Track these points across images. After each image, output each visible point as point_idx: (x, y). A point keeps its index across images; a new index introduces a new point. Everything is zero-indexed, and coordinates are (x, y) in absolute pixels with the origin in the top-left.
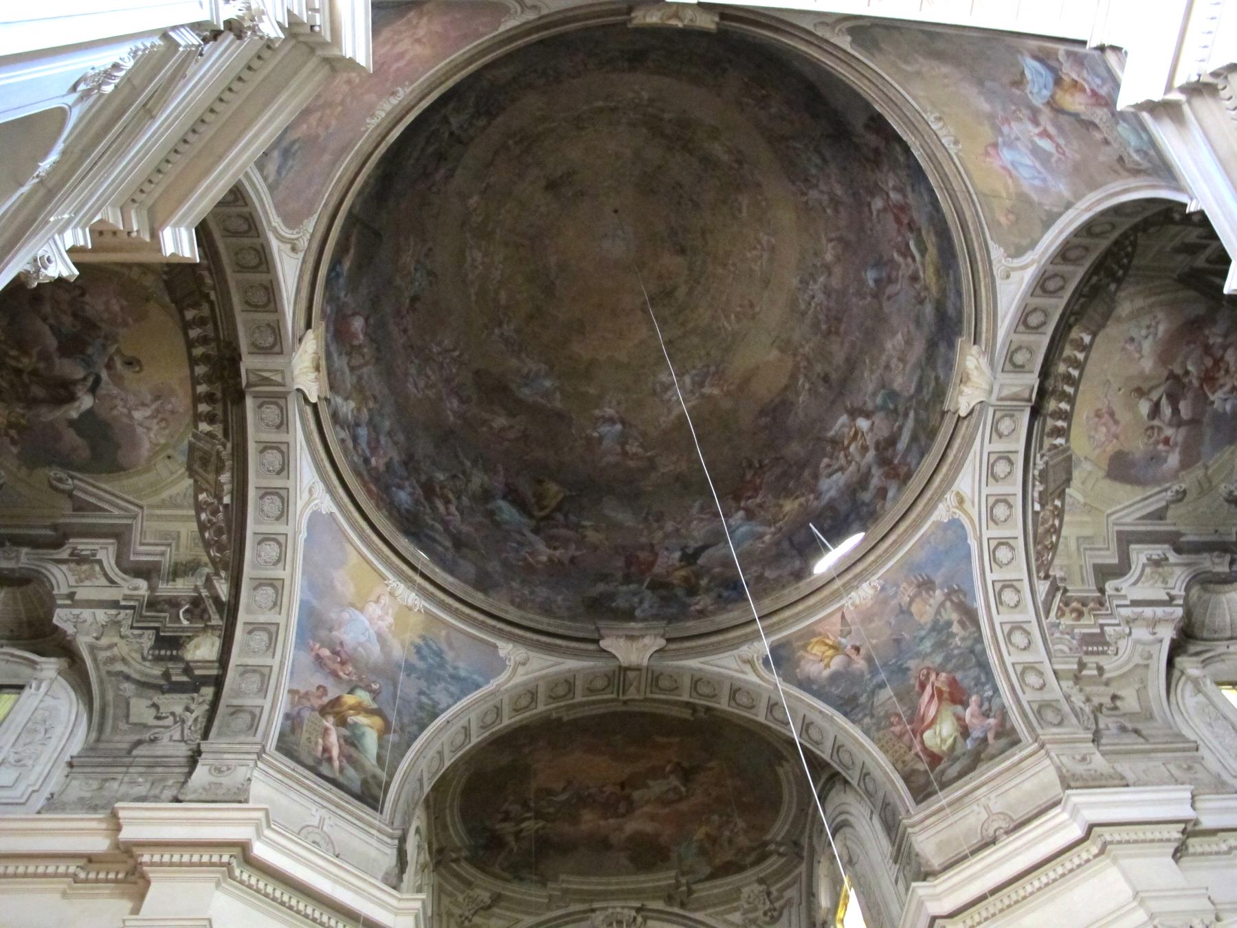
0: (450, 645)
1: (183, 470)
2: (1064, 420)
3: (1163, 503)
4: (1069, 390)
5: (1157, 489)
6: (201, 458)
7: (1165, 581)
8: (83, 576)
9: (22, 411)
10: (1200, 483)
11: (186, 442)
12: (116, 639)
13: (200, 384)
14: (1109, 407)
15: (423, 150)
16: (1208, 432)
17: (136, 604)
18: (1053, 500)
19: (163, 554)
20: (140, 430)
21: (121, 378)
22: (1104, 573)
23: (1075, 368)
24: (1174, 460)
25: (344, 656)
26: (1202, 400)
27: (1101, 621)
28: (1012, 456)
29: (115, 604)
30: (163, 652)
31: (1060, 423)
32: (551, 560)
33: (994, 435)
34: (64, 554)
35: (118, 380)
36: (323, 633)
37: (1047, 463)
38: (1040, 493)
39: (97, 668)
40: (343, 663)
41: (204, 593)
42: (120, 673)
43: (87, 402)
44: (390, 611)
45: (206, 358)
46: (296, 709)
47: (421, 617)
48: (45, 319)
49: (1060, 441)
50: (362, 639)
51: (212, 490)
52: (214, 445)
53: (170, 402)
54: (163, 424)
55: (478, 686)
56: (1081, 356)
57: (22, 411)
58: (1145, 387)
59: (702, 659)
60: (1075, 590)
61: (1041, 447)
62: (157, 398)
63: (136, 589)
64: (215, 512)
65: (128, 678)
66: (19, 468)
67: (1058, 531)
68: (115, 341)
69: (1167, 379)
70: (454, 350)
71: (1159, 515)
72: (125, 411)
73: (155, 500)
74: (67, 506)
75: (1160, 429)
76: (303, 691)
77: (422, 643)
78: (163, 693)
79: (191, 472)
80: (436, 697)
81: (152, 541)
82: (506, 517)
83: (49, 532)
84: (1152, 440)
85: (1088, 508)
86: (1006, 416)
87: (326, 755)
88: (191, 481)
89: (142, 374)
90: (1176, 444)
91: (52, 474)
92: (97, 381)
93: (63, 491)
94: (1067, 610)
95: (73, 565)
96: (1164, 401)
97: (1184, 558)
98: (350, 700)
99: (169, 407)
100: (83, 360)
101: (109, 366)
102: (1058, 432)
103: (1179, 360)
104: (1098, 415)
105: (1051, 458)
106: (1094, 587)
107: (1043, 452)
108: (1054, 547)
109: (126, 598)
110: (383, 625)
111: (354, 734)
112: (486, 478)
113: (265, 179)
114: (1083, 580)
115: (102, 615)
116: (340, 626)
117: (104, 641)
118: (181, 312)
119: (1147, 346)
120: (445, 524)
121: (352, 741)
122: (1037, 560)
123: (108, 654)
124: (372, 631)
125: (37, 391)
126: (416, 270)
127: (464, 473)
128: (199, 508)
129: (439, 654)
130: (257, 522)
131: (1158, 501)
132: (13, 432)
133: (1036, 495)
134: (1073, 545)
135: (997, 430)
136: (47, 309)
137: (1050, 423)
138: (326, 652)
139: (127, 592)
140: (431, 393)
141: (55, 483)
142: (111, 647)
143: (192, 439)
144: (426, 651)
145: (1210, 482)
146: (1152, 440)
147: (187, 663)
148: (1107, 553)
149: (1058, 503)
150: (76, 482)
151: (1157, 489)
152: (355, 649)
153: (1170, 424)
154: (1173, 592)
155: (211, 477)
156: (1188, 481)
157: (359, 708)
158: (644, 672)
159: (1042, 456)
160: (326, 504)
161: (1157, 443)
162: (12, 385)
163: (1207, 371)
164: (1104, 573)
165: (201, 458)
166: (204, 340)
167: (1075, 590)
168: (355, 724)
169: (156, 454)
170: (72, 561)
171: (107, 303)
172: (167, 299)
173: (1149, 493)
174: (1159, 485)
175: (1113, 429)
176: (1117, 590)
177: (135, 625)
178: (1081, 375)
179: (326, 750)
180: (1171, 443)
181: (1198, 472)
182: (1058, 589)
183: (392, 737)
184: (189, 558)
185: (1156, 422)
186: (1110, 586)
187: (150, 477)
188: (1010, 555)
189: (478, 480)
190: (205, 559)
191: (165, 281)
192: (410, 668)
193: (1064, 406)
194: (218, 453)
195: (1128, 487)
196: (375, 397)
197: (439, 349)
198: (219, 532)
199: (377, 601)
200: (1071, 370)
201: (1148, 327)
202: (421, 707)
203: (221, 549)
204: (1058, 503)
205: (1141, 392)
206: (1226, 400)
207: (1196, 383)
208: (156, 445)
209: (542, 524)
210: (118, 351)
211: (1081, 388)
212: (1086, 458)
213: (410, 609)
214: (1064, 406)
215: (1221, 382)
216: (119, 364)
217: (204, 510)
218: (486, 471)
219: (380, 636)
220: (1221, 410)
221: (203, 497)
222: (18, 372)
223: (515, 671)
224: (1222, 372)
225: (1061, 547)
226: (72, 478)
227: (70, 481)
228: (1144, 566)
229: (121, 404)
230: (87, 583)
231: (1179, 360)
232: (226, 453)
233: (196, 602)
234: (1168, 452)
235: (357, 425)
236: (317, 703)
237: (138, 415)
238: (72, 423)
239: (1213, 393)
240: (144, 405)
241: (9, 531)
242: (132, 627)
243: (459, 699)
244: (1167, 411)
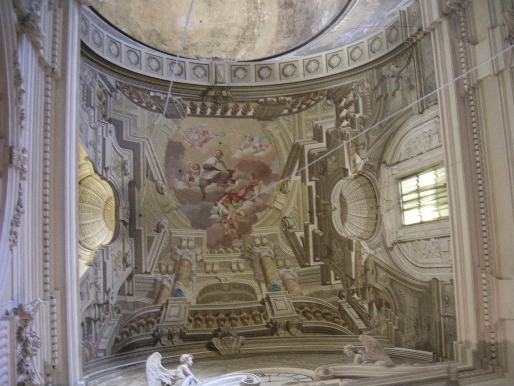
2: (201, 112)
3: (156, 178)
4: (218, 113)
5: (163, 175)
7: (114, 169)
10: (167, 205)
14: (210, 138)
16: (197, 207)
18: (156, 105)
22: (119, 126)
23: (232, 113)
24: (181, 185)
26: (216, 197)
27: (96, 110)
28: (183, 76)
31: (199, 110)
33: (194, 65)
37: (176, 103)
38: (159, 97)
49: (189, 111)
56: (239, 114)
58: (223, 159)
60: (110, 101)
61: (184, 99)
67: (139, 104)
69: (229, 171)
71: (150, 176)
75: (198, 174)
84: (191, 169)
85: (151, 127)
86: (205, 71)
90: (190, 186)
94: (102, 90)
96: (216, 172)
97: (126, 188)
102: (193, 109)
103: (241, 173)
104: (205, 133)
105: (179, 106)
106: (112, 116)
107: (182, 101)
108: (131, 99)
114: (114, 110)
119: (251, 150)
122: (125, 84)
131: (157, 175)
133: (158, 94)
134: (132, 112)
135: (197, 67)
137: (198, 104)
145: (168, 212)
146: (191, 169)
148: (129, 135)
149: (154, 107)
151: (163, 175)
153: (202, 179)
154: (109, 171)
156: (169, 196)
159: (179, 100)
161: (190, 172)
163: (236, 194)
164: (119, 126)
167: (110, 101)
173: (161, 168)
174: (165, 176)
175: (197, 143)
176: (110, 132)
178: (228, 117)
180: (191, 182)
181: (174, 203)
182: (112, 91)
185: (202, 170)
186: (111, 127)
188: (133, 61)
193: (209, 111)
195: (164, 155)
200: (231, 110)
201: (261, 146)
204: (154, 107)
205: (220, 156)
206: (219, 213)
207: (227, 190)
211: (220, 119)
212: (179, 127)
214: (209, 111)
215: (230, 206)
220: (212, 212)
224: (235, 204)
225: (132, 104)
228: (122, 157)
231: (241, 173)
234: (185, 181)
239: (223, 204)
244: (210, 176)
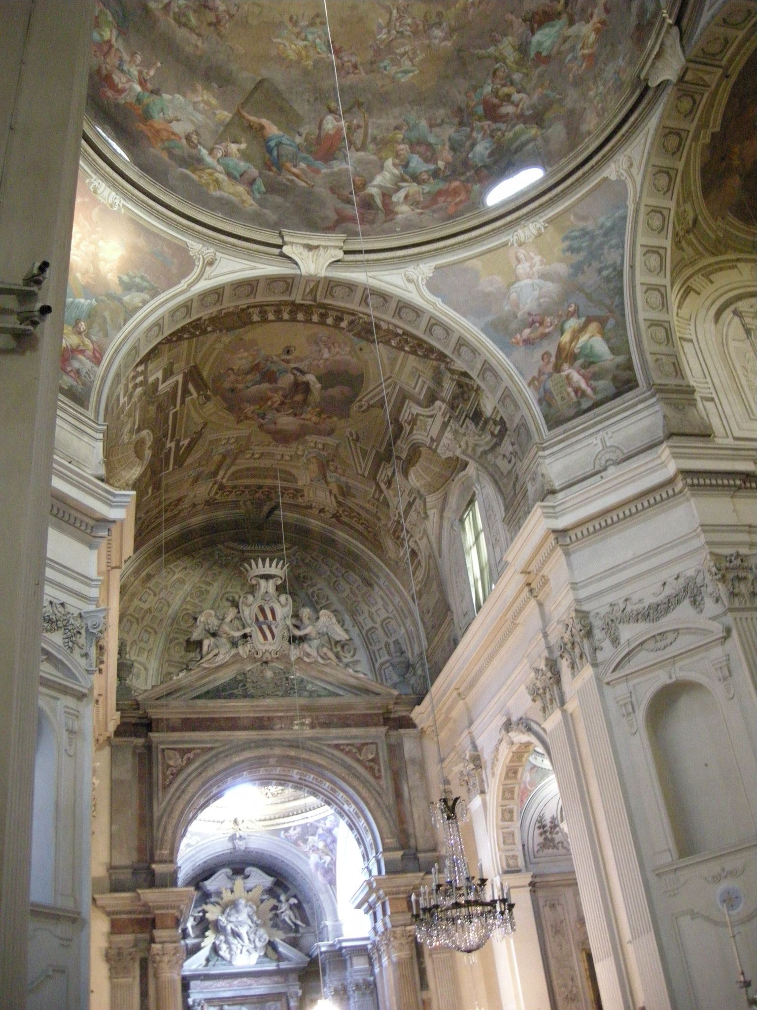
0: (584, 218)
6: (367, 333)
12: (465, 439)
13: (311, 319)
15: (192, 30)
19: (424, 382)
20: (337, 357)
21: (296, 357)
25: (537, 318)
32: (597, 31)
34: (407, 428)
36: (513, 326)
40: (541, 323)
44: (532, 254)
46: (542, 389)
47: (551, 228)
50: (536, 293)
52: (358, 323)
54: (336, 345)
55: (624, 218)
59: (706, 8)
63: (440, 408)
64: (407, 342)
70: (391, 14)
72: (322, 361)
74: (377, 411)
76: (536, 374)
77: (567, 243)
80: (610, 262)
82: (548, 43)
87: (579, 394)
92: (297, 369)
98: (566, 338)
101: (288, 362)
110: (538, 267)
111: (586, 356)
112: (510, 38)
113: (145, 302)
115: (448, 435)
116: (517, 306)
120: (521, 117)
121: (588, 361)
124: (537, 281)
126: (305, 39)
127: (497, 60)
128: (401, 349)
129: (585, 233)
130: (417, 328)
132: (323, 416)
138: (527, 332)
140: (421, 56)
142: (467, 444)
144: (576, 244)
152: (540, 305)
157: (575, 337)
158: (691, 65)
160: (425, 269)
162: (293, 408)
168: (581, 348)
179: (577, 390)
183: (611, 323)
189: (507, 47)
192: (578, 268)
196: (397, 128)
197: (385, 31)
199: (519, 261)
202: (608, 280)
209: (569, 9)
210: (277, 356)
213: (540, 235)
216: (288, 357)
218: (505, 35)
219: (544, 276)
221: (393, 343)
222: (283, 403)
223: (631, 176)
226: (361, 400)
230: (428, 428)
235: (406, 166)
236: (550, 368)
237: (326, 355)
238: (324, 388)
240: (320, 351)
242: (462, 426)
243: (623, 242)
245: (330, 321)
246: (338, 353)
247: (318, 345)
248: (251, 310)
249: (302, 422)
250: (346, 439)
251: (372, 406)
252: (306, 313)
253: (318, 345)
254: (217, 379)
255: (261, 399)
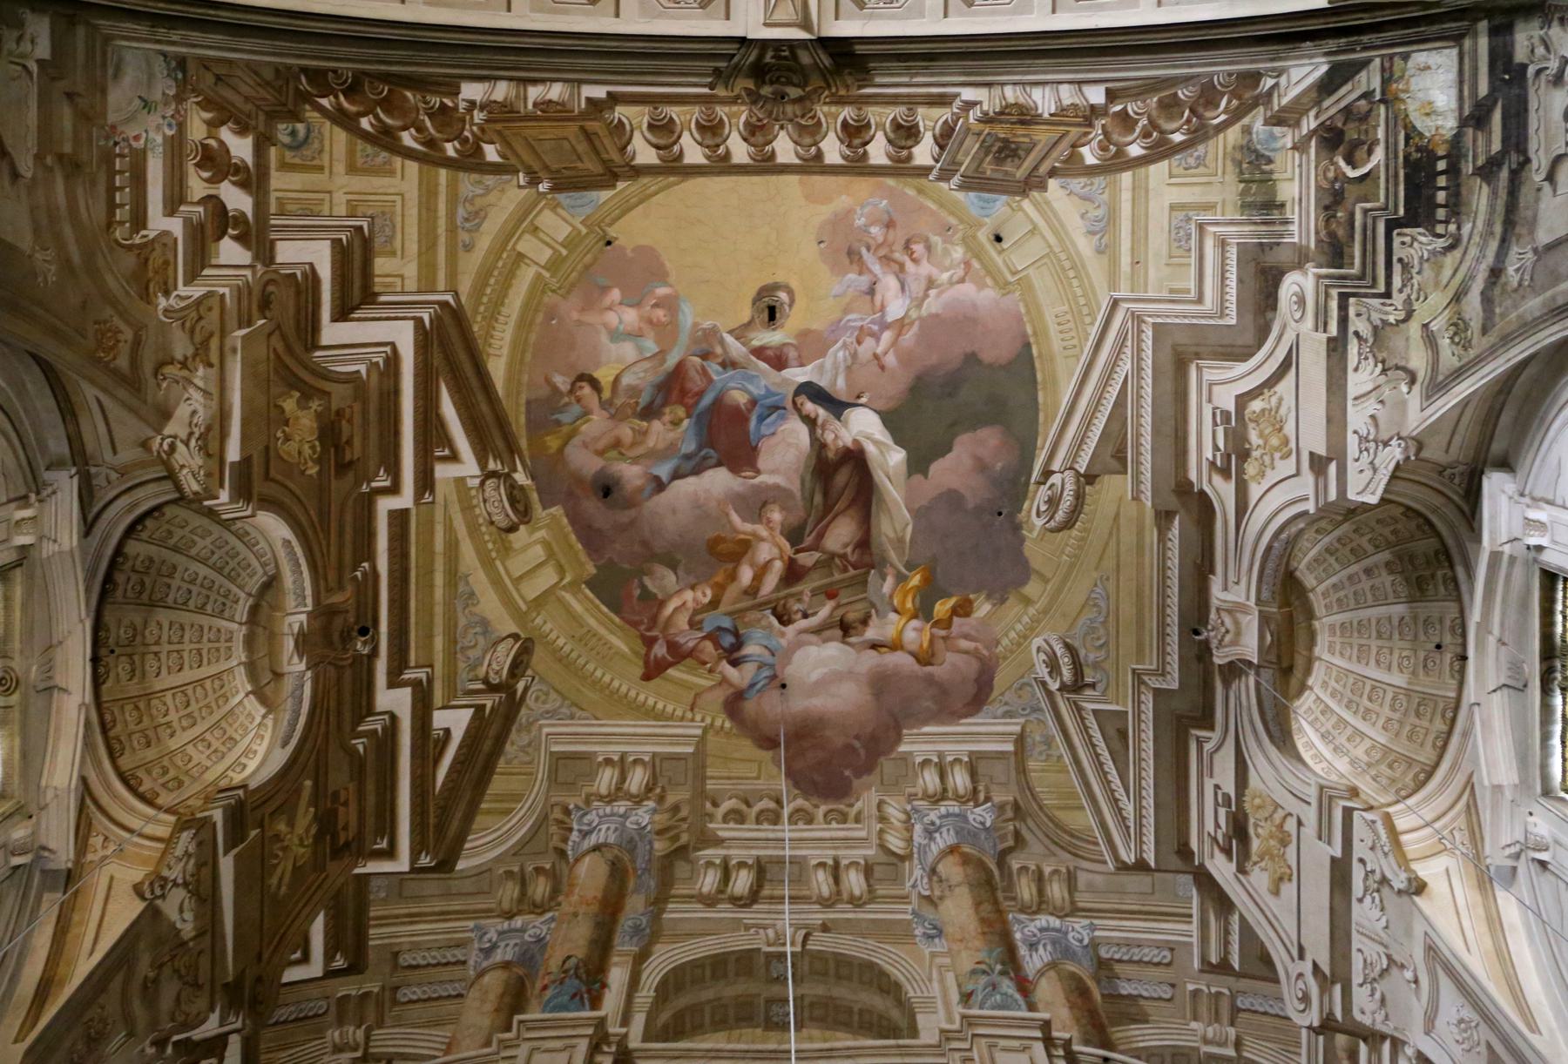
1: (1026, 204)
6: (999, 160)
8: (1275, 441)
9: (890, 581)
11: (960, 196)
12: (1414, 328)
13: (819, 155)
17: (1334, 293)
19: (1222, 244)
20: (933, 305)
21: (804, 334)
29: (1337, 347)
30: (1441, 197)
34: (1223, 492)
35: (812, 345)
39: (1478, 361)
41: (1310, 123)
42: (1487, 300)
43: (863, 426)
45: (754, 132)
48: (660, 486)
51: (1075, 131)
52: (967, 130)
53: (865, 230)
54: (918, 248)
57: (890, 581)
62: (853, 255)
63: (1301, 301)
64: (1126, 121)
65: (1496, 273)
66: (1028, 601)
68: (712, 334)
72: (887, 336)
73: (1096, 270)
74: (1114, 488)
78: (1528, 161)
79: (1032, 184)
81: (1193, 271)
83: (1175, 531)
88: (1053, 184)
89: (794, 284)
91: (1039, 522)
92: (812, 391)
93: (1079, 497)
95: (1251, 468)
99: (874, 230)
100: (761, 419)
101: (778, 361)
109: (1321, 323)
115: (1361, 379)
117: (1418, 360)
118: (638, 172)
123: (1444, 342)
125: (841, 534)
128: (1115, 163)
132: (942, 608)
136: (631, 474)
139: (1309, 322)
141: (1060, 516)
142: (1430, 339)
143: (956, 179)
147: (1463, 123)
150: (1056, 466)
155: (1043, 136)
162: (831, 596)
165: (999, 160)
166: (711, 130)
169: (991, 271)
170: (1241, 471)
171: (616, 335)
172: (605, 195)
177: (1382, 288)
184: (1231, 177)
187: (1043, 283)
190: (1233, 134)
191: (556, 188)
194: (986, 119)
198: (1170, 106)
203: (1209, 96)
208: (967, 264)
210: (740, 333)
217: (1120, 152)
221: (1089, 156)
222: (793, 573)
226: (1047, 473)
227: (1055, 479)
229: (869, 342)
230: (1289, 428)
232: (985, 99)
233: (1332, 139)
237: (896, 308)
238: (918, 464)
240: (871, 291)
241: (1173, 632)
242: (1387, 295)
245: (878, 151)
246: (931, 283)
247: (863, 269)
248: (621, 112)
249: (870, 659)
250: (1039, 693)
251: (1090, 478)
252: (802, 129)
253: (863, 269)
254: (545, 412)
255: (713, 545)
